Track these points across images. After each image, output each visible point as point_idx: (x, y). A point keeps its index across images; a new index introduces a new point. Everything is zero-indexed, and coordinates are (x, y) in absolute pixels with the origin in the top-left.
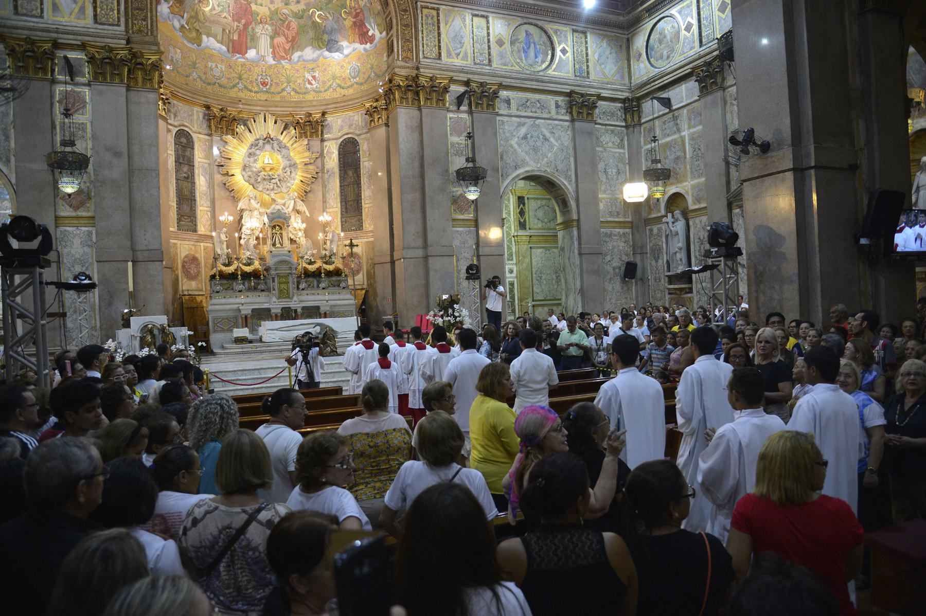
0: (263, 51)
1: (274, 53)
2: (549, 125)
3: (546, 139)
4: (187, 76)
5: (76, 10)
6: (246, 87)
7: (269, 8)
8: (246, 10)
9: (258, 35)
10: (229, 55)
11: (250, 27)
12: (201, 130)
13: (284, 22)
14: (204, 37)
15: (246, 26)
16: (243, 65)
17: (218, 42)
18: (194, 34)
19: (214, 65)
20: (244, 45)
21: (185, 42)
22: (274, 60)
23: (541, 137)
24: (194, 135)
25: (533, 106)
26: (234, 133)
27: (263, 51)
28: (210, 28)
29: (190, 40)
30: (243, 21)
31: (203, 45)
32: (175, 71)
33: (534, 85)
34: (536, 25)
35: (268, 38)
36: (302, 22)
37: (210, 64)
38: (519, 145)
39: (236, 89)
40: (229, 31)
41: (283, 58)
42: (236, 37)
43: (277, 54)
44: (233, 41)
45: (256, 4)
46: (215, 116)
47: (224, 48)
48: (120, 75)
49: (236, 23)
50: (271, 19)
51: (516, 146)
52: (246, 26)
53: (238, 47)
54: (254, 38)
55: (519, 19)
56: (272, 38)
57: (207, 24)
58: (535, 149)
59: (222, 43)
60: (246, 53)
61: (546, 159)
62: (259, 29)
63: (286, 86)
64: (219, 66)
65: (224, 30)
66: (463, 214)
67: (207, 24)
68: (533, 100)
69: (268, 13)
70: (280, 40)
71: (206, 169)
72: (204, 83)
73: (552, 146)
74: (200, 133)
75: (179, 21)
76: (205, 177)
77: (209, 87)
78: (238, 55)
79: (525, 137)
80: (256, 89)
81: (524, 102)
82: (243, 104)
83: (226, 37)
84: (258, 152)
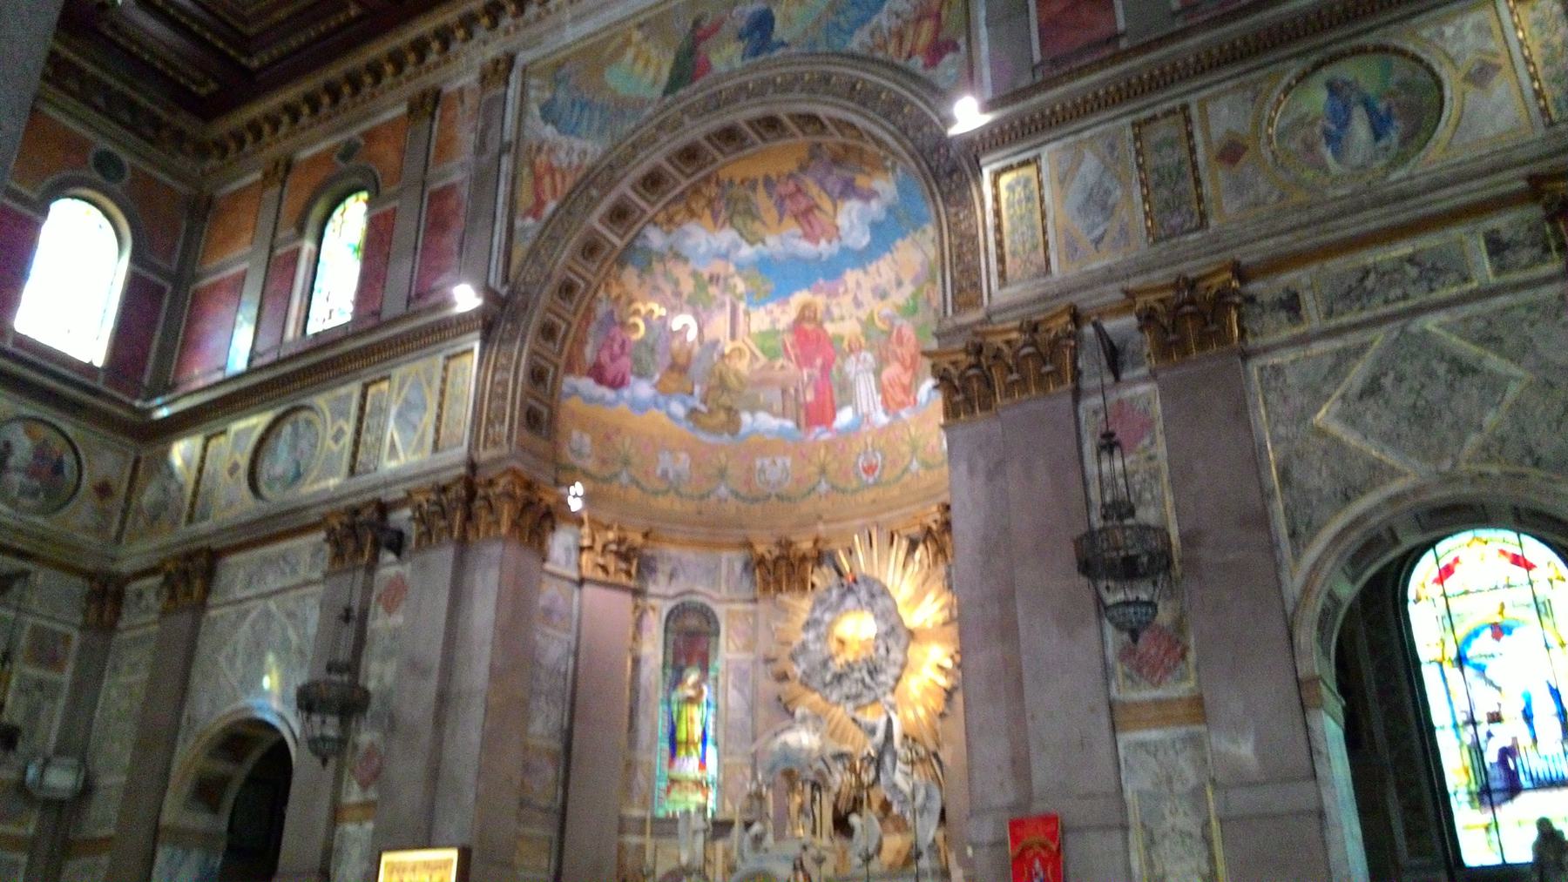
0: (864, 403)
1: (885, 402)
2: (1466, 320)
3: (1462, 368)
4: (702, 497)
5: (414, 443)
6: (834, 487)
7: (859, 319)
8: (818, 339)
9: (852, 377)
10: (799, 435)
11: (834, 369)
12: (735, 596)
13: (889, 334)
14: (746, 418)
15: (826, 369)
16: (828, 445)
17: (775, 415)
18: (722, 416)
19: (767, 462)
20: (828, 404)
21: (703, 437)
22: (887, 413)
23: (1441, 369)
24: (720, 610)
25: (1391, 284)
26: (803, 585)
27: (864, 403)
28: (757, 397)
29: (714, 430)
30: (819, 362)
31: (743, 430)
32: (672, 493)
33: (1374, 220)
34: (1361, 51)
35: (872, 377)
36: (919, 318)
37: (758, 463)
38: (1351, 420)
39: (813, 496)
40: (796, 390)
41: (902, 405)
42: (810, 396)
43: (892, 404)
44: (807, 407)
45: (832, 320)
46: (761, 561)
47: (789, 424)
48: (450, 529)
49: (805, 372)
50: (868, 338)
51: (1336, 428)
52: (826, 369)
53: (819, 414)
54: (847, 392)
55: (1292, 63)
56: (877, 373)
57: (748, 391)
58: (1422, 417)
59: (784, 415)
60: (834, 417)
61: (1474, 439)
62: (851, 366)
63: (911, 461)
64: (779, 462)
65: (784, 392)
66: (1157, 685)
67: (748, 391)
68: (1388, 267)
69: (858, 329)
70: (892, 371)
71: (745, 673)
72: (744, 499)
73: (1496, 385)
74: (732, 601)
75: (684, 403)
76: (741, 691)
77: (758, 507)
78: (818, 430)
79: (1372, 389)
80: (854, 484)
81: (1352, 281)
82: (826, 522)
83: (790, 404)
84: (827, 617)
